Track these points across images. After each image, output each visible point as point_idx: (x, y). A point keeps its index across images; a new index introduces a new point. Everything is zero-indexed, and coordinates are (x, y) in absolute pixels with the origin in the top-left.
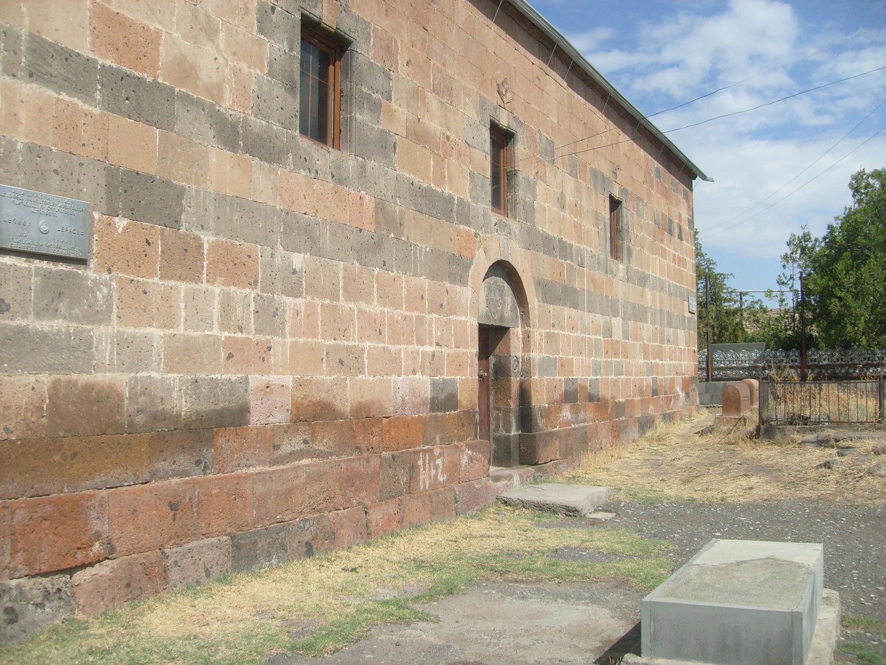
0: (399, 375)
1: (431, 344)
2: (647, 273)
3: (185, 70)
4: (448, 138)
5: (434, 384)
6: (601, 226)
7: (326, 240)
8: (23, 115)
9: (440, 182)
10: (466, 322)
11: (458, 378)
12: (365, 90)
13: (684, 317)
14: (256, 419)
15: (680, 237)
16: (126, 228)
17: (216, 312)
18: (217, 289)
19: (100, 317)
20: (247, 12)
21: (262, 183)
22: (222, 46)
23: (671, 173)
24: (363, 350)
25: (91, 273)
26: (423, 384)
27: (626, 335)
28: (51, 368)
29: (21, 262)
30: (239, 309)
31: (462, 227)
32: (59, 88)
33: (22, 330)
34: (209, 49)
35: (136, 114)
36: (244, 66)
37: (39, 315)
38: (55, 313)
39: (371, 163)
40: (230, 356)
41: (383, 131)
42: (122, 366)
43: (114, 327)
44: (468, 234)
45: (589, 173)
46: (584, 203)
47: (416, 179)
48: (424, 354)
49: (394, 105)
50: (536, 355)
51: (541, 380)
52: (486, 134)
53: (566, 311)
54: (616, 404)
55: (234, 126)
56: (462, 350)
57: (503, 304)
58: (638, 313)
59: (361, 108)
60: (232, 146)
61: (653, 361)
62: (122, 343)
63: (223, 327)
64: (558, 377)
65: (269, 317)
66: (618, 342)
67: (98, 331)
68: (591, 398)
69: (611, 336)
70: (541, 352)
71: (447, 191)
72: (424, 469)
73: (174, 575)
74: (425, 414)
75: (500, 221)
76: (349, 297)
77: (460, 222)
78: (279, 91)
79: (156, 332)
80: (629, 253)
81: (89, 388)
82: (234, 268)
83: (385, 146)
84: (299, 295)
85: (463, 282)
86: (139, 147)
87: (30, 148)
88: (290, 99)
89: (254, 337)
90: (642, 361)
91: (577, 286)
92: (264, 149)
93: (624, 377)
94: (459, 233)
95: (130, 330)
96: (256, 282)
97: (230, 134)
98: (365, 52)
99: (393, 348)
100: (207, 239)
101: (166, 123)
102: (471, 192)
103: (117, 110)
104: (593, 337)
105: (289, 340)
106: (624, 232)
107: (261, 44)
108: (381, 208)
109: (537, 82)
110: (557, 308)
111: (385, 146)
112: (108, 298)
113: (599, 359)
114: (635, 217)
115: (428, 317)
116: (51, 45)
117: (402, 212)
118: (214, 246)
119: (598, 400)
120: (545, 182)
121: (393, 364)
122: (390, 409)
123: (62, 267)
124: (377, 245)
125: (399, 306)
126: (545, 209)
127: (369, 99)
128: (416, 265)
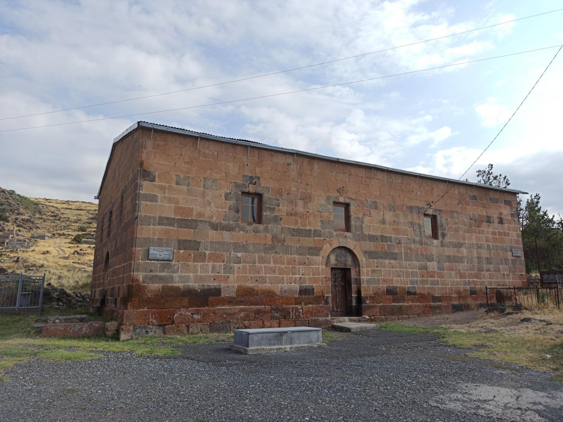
0: (283, 284)
1: (299, 275)
2: (462, 241)
3: (200, 214)
4: (308, 212)
5: (301, 287)
6: (417, 226)
7: (251, 248)
8: (157, 233)
9: (306, 225)
10: (319, 268)
11: (314, 285)
12: (267, 206)
13: (508, 259)
14: (222, 295)
15: (501, 221)
16: (183, 253)
17: (210, 269)
18: (210, 264)
19: (177, 271)
20: (221, 196)
21: (227, 236)
22: (213, 207)
23: (489, 194)
24: (266, 277)
25: (173, 263)
26: (296, 287)
27: (441, 268)
28: (162, 283)
29: (156, 262)
30: (218, 268)
31: (316, 238)
32: (166, 225)
33: (156, 276)
34: (208, 208)
35: (187, 227)
36: (220, 210)
37: (159, 272)
38: (164, 272)
39: (269, 226)
40: (215, 279)
41: (275, 216)
42: (181, 282)
43: (179, 274)
44: (320, 240)
45: (405, 208)
46: (402, 220)
47: (292, 227)
48: (295, 278)
49: (281, 207)
50: (364, 277)
51: (368, 287)
52: (331, 207)
53: (387, 261)
54: (432, 297)
55: (217, 224)
56: (316, 276)
57: (346, 261)
58: (460, 260)
59: (266, 211)
60: (216, 229)
61: (470, 280)
62: (181, 277)
63: (212, 273)
64: (381, 285)
65: (229, 270)
66: (434, 272)
67: (175, 275)
68: (409, 293)
69: (426, 269)
70: (368, 275)
71: (308, 228)
72: (293, 312)
73: (191, 330)
74: (297, 296)
75: (339, 235)
76: (259, 263)
77: (314, 236)
78: (233, 213)
79: (191, 275)
80: (444, 235)
81: (172, 286)
82: (215, 258)
83: (277, 220)
84: (240, 263)
85: (317, 255)
86: (187, 234)
87: (158, 239)
88: (237, 214)
89: (222, 274)
90: (458, 280)
91: (396, 251)
92: (228, 228)
93: (440, 286)
94: (314, 240)
95: (183, 274)
96: (224, 261)
97: (215, 227)
98: (266, 196)
99: (280, 276)
100: (207, 252)
101: (195, 228)
102: (321, 227)
103: (181, 227)
104: (410, 270)
105: (236, 275)
106: (439, 228)
107: (226, 203)
108: (274, 237)
109: (365, 183)
110: (380, 260)
111: (277, 220)
112: (178, 268)
113: (415, 279)
114: (449, 219)
115: (298, 267)
116: (165, 217)
117: (284, 238)
118: (209, 254)
119: (415, 294)
120: (370, 216)
121: (282, 281)
122: (279, 294)
123: (166, 262)
124: (273, 248)
125: (283, 264)
126: (370, 226)
127: (269, 208)
128: (291, 252)
